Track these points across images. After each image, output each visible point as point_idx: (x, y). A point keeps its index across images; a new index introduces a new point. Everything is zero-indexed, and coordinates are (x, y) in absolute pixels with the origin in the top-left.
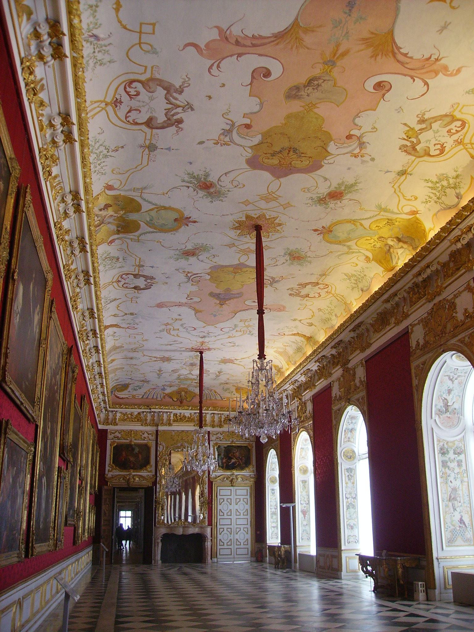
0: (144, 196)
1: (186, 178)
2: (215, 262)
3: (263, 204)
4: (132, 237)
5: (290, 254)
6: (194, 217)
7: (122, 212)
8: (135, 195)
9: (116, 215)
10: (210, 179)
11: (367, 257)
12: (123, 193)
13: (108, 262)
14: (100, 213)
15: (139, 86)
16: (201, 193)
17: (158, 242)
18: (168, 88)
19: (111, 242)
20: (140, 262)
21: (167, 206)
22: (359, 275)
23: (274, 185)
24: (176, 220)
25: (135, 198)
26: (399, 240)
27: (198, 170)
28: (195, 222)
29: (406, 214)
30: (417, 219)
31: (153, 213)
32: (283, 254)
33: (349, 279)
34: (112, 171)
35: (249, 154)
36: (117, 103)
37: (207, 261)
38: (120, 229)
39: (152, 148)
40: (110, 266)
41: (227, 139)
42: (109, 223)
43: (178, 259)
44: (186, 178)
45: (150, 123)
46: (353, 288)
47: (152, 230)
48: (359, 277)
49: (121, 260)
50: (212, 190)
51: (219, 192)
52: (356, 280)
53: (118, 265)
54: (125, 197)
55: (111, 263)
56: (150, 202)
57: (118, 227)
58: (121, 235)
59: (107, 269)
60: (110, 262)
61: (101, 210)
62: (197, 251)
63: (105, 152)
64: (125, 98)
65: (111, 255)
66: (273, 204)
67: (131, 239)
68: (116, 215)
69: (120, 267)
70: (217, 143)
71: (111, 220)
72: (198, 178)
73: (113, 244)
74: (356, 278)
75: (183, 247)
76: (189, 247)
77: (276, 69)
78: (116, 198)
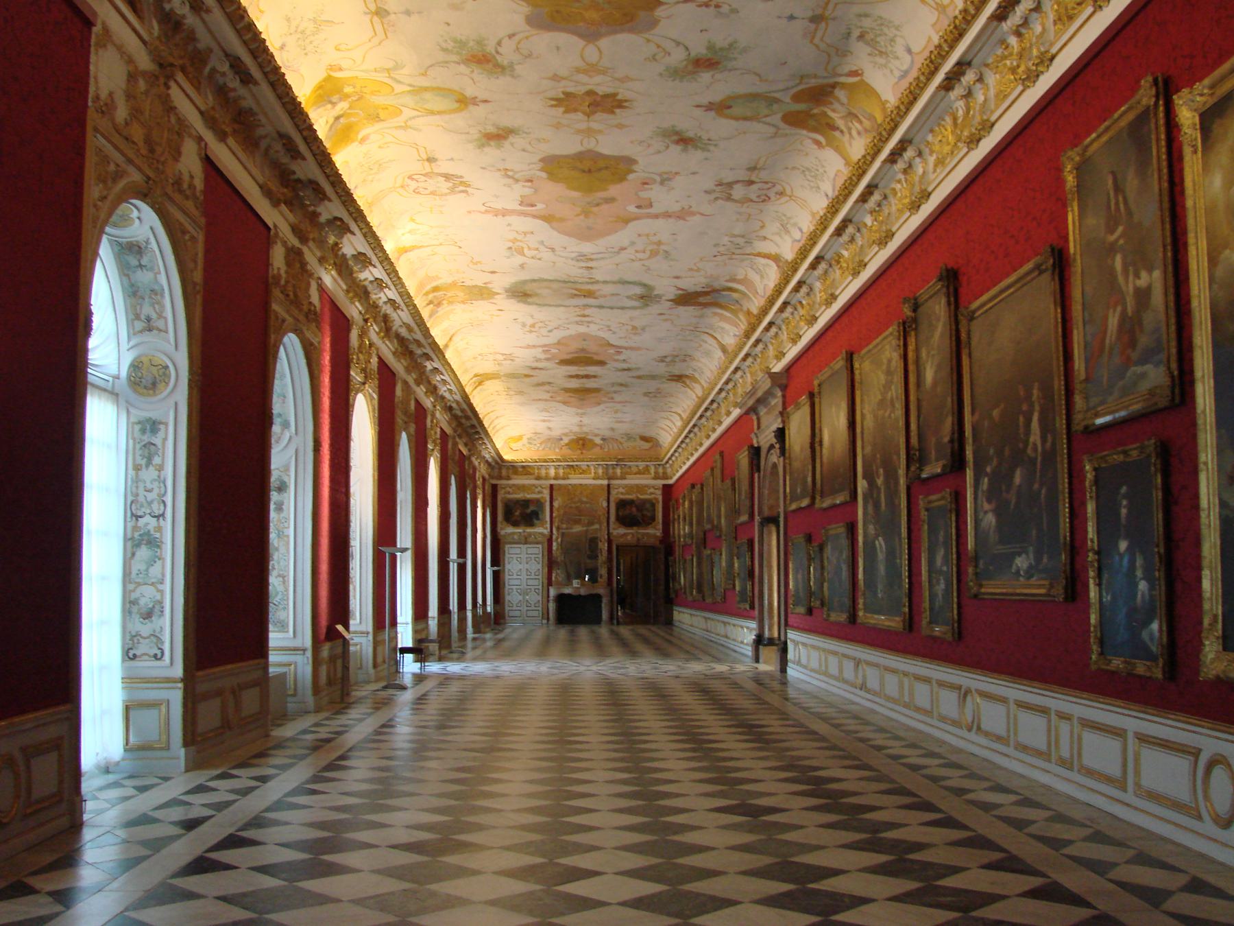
0: (772, 130)
1: (712, 148)
2: (648, 41)
3: (594, 125)
4: (813, 81)
5: (503, 68)
6: (699, 112)
7: (815, 111)
8: (787, 129)
9: (826, 110)
10: (679, 148)
11: (341, 69)
12: (804, 132)
13: (882, 44)
14: (845, 130)
15: (755, 199)
16: (690, 134)
17: (766, 81)
18: (729, 198)
19: (854, 73)
20: (816, 30)
21: (741, 122)
22: (311, 42)
23: (590, 144)
24: (729, 107)
25: (787, 126)
26: (337, 118)
27: (695, 156)
28: (698, 106)
29: (369, 134)
30: (353, 142)
31: (766, 112)
32: (516, 67)
33: (314, 21)
34: (807, 154)
35: (635, 167)
36: (781, 194)
37: (669, 46)
38: (830, 89)
39: (753, 169)
40: (886, 30)
41: (665, 176)
42: (843, 104)
43: (731, 45)
44: (712, 148)
45: (751, 183)
46: (288, 20)
47: (776, 95)
48: (307, 41)
49: (856, 33)
50: (675, 138)
51: (664, 136)
52: (303, 32)
53: (867, 23)
54: (804, 128)
55: (880, 35)
56: (769, 124)
57: (832, 92)
58: (831, 81)
59: (893, 30)
60: (878, 39)
61: (842, 132)
62: (690, 68)
63: (807, 173)
64: (772, 194)
65: (869, 50)
66: (583, 126)
67: (815, 76)
68: (826, 110)
69: (866, 15)
70: (676, 173)
71: (836, 106)
72: (696, 147)
73: (854, 68)
74: (308, 32)
75: (718, 76)
76: (706, 76)
77: (632, 209)
78: (815, 130)
